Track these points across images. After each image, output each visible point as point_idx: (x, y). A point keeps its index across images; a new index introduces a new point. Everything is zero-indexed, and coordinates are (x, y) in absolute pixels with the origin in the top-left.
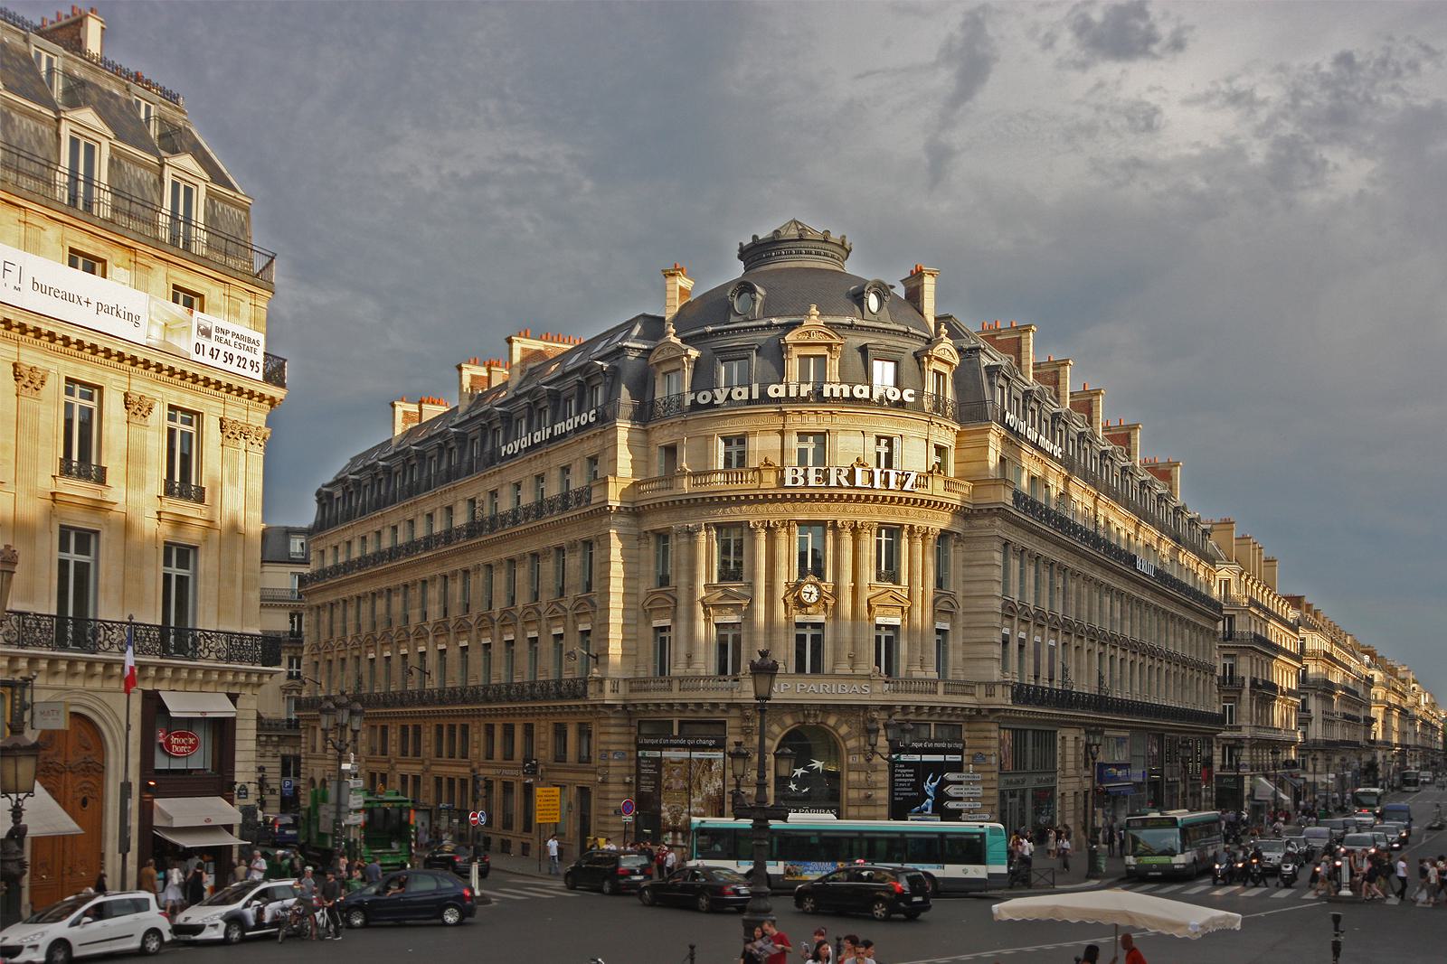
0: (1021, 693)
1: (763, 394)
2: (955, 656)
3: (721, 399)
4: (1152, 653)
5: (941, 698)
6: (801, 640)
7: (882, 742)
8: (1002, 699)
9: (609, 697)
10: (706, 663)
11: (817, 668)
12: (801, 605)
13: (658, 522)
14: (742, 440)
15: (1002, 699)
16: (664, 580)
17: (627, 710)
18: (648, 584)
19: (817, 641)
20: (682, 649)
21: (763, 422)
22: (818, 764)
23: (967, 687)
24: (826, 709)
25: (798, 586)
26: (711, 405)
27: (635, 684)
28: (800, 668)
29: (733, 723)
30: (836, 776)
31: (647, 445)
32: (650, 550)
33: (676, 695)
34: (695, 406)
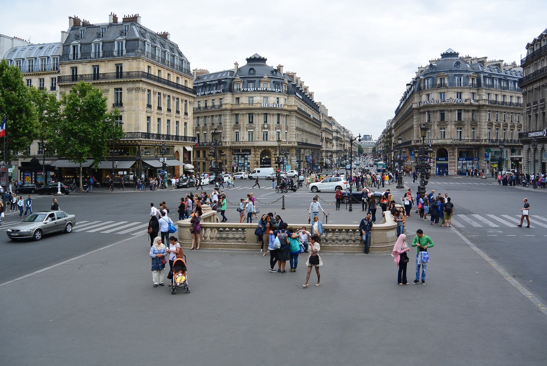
0: (298, 143)
1: (257, 89)
2: (288, 137)
3: (249, 90)
4: (312, 134)
5: (287, 144)
6: (264, 134)
7: (278, 152)
8: (296, 145)
9: (228, 145)
10: (246, 138)
11: (267, 139)
12: (264, 128)
13: (237, 112)
14: (252, 97)
15: (296, 145)
16: (237, 123)
17: (231, 148)
18: (234, 123)
19: (267, 134)
20: (242, 136)
21: (256, 95)
22: (267, 157)
23: (290, 142)
24: (269, 147)
25: (264, 125)
26: (247, 91)
27: (233, 143)
28: (264, 139)
29: (252, 150)
30: (270, 159)
31: (233, 97)
32: (234, 117)
33: (242, 145)
34: (243, 90)
